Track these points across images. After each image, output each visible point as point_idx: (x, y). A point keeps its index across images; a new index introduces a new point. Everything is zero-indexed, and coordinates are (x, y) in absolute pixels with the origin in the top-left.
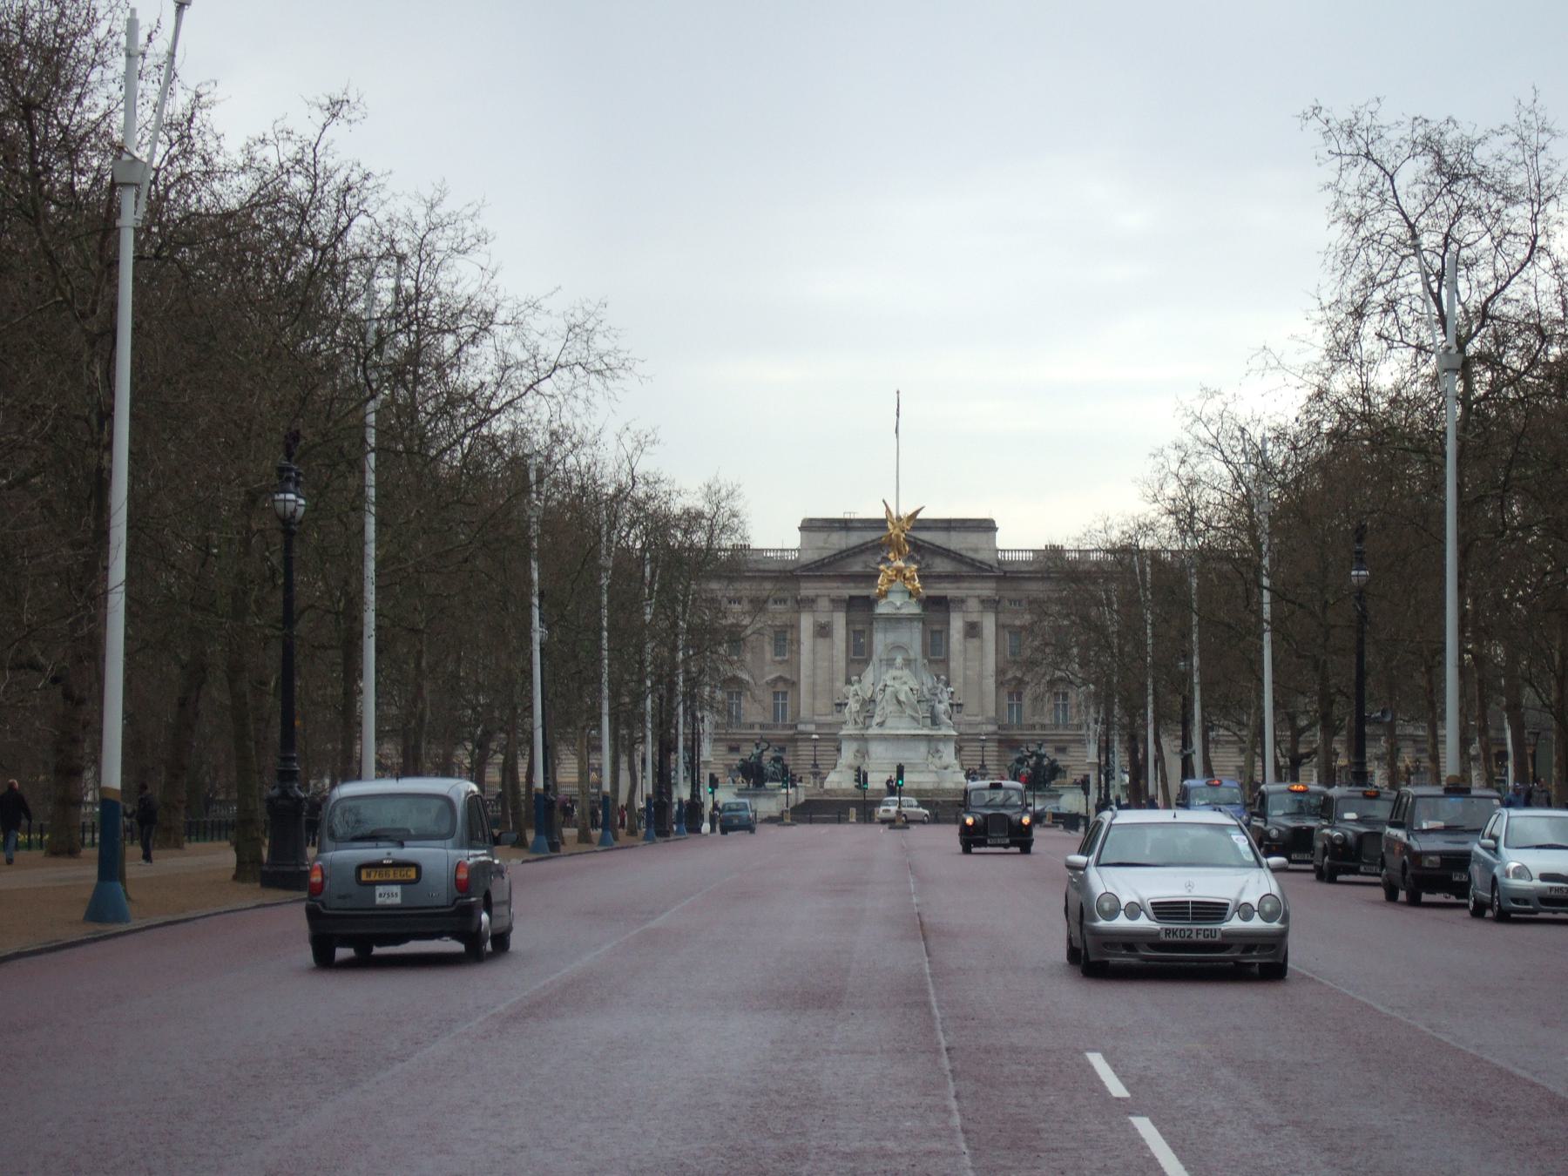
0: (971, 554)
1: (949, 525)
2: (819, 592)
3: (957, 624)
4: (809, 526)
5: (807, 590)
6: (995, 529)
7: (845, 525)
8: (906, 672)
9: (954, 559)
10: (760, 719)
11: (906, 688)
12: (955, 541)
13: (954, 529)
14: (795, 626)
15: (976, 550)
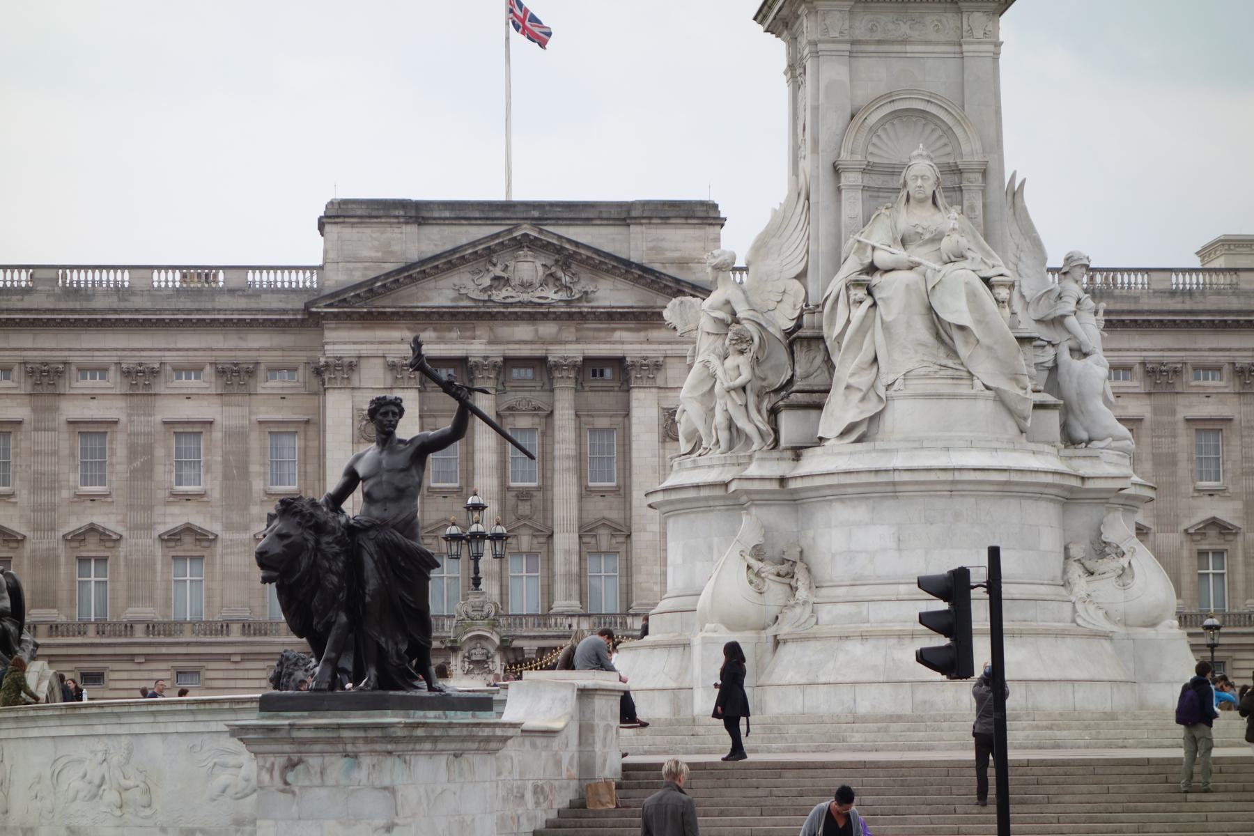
0: (672, 271)
1: (624, 215)
2: (365, 350)
3: (644, 408)
4: (340, 214)
5: (341, 342)
6: (720, 222)
7: (416, 213)
8: (948, 219)
9: (637, 280)
10: (245, 614)
11: (964, 275)
12: (636, 244)
13: (637, 220)
14: (313, 425)
15: (683, 263)
